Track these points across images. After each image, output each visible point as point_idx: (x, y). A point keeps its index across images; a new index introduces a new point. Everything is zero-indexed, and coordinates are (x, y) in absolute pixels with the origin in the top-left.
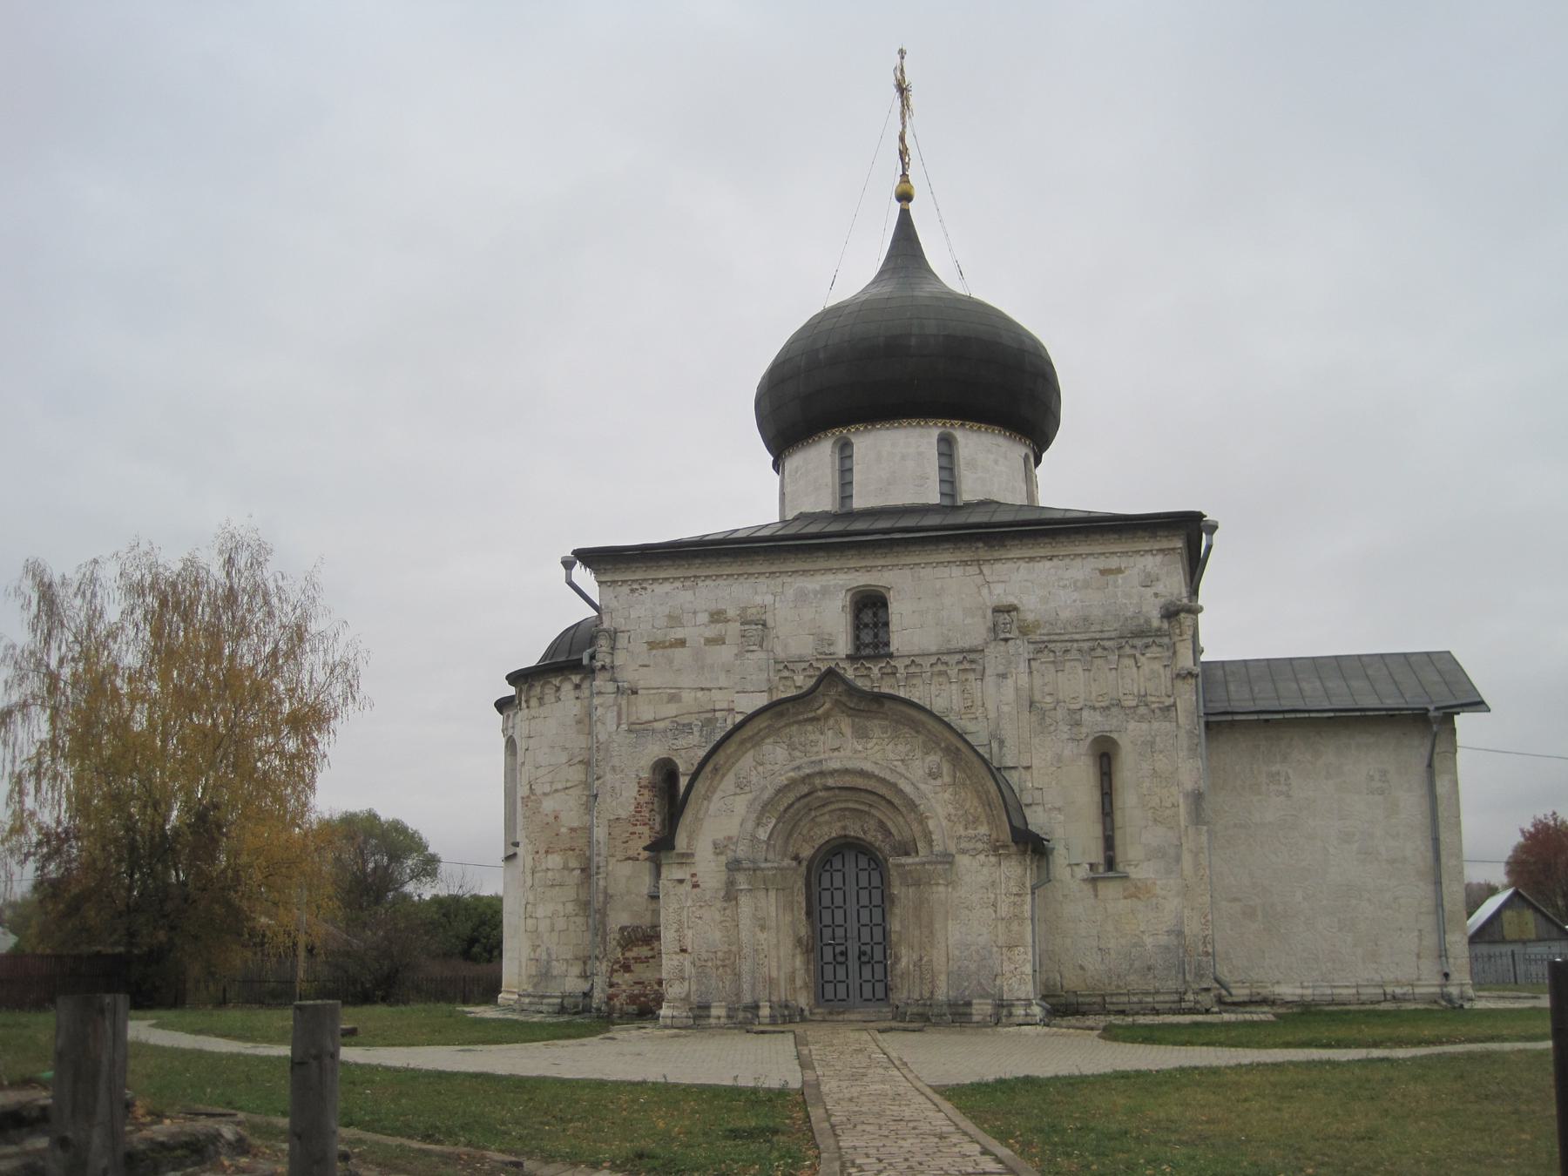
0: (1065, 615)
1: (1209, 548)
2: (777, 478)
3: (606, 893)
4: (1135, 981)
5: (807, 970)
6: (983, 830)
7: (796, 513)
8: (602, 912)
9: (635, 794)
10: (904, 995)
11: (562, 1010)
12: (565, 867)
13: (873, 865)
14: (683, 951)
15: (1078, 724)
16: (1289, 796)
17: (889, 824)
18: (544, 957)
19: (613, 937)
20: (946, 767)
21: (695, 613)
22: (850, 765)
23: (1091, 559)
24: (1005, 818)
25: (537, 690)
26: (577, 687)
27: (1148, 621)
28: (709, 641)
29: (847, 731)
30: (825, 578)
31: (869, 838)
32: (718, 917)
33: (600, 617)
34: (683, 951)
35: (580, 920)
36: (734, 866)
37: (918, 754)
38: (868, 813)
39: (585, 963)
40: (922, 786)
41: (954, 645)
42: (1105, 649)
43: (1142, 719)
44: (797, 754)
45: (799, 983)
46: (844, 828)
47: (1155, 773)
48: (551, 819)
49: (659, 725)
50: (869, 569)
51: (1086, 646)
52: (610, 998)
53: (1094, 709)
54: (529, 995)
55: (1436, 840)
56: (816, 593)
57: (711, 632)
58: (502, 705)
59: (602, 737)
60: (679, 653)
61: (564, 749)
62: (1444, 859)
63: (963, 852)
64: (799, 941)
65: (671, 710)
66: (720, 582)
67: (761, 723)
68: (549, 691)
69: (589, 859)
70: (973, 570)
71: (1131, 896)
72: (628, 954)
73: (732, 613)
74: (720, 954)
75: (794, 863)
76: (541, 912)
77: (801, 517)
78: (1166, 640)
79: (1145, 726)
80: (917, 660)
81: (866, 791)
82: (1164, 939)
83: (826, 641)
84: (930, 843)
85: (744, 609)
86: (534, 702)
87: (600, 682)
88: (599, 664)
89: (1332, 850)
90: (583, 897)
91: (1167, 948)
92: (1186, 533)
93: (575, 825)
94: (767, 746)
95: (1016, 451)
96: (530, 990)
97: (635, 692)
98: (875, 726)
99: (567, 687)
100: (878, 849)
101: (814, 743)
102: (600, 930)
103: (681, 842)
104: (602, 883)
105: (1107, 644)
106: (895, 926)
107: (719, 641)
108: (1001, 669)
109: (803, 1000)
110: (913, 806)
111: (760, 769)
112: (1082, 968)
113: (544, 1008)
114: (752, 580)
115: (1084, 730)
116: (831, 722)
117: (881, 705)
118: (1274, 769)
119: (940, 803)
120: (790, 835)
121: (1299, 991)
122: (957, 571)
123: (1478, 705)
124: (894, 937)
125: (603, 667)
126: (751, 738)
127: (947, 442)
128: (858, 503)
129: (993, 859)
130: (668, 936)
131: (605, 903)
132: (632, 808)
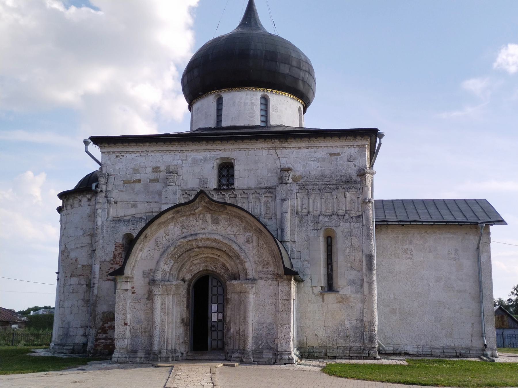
0: (313, 173)
1: (380, 144)
2: (190, 113)
3: (97, 296)
4: (341, 343)
5: (186, 334)
6: (271, 268)
7: (197, 128)
8: (94, 305)
9: (114, 250)
10: (231, 347)
11: (73, 352)
12: (79, 284)
13: (219, 284)
14: (126, 324)
15: (318, 222)
16: (411, 259)
17: (228, 265)
19: (99, 317)
20: (255, 238)
21: (146, 168)
22: (209, 236)
23: (326, 148)
24: (281, 263)
25: (71, 201)
26: (89, 200)
27: (351, 177)
28: (152, 181)
29: (209, 220)
30: (206, 153)
31: (218, 271)
32: (143, 308)
33: (101, 169)
34: (126, 324)
35: (85, 309)
36: (153, 282)
37: (242, 232)
38: (218, 260)
39: (85, 330)
40: (243, 247)
41: (262, 185)
42: (330, 189)
43: (347, 221)
44: (185, 230)
45: (181, 341)
46: (206, 266)
47: (352, 246)
48: (74, 261)
49: (127, 218)
50: (225, 150)
51: (322, 187)
52: (96, 346)
53: (325, 216)
55: (480, 282)
56: (201, 160)
57: (153, 176)
58: (59, 210)
59: (99, 223)
60: (138, 186)
61: (82, 228)
62: (484, 291)
63: (261, 278)
64: (183, 320)
65: (132, 211)
66: (158, 154)
67: (169, 215)
68: (76, 201)
69: (90, 280)
70: (272, 152)
71: (340, 302)
72: (106, 325)
73: (163, 168)
74: (143, 326)
75: (182, 283)
77: (199, 129)
78: (359, 186)
79: (348, 224)
80: (245, 191)
81: (217, 249)
82: (354, 322)
83: (203, 181)
84: (246, 274)
85: (168, 167)
86: (69, 207)
87: (101, 198)
88: (100, 190)
89: (431, 285)
90: (86, 298)
91: (356, 327)
92: (369, 136)
93: (85, 264)
94: (171, 226)
95: (296, 104)
97: (117, 203)
98: (222, 218)
99: (85, 200)
100: (222, 276)
101: (194, 226)
102: (93, 314)
103: (128, 271)
104: (96, 291)
105: (331, 186)
106: (228, 313)
107: (156, 180)
108: (284, 196)
109: (183, 349)
110: (238, 256)
111: (167, 237)
112: (316, 335)
113: (64, 351)
114: (172, 153)
115: (319, 225)
116: (202, 216)
117: (226, 209)
118: (406, 247)
119: (252, 256)
120: (181, 269)
121: (416, 350)
122: (265, 152)
123: (501, 221)
124: (228, 319)
125: (101, 191)
126: (163, 223)
127: (265, 101)
128: (224, 124)
129: (275, 283)
130: (118, 317)
131: (96, 301)
132: (112, 256)
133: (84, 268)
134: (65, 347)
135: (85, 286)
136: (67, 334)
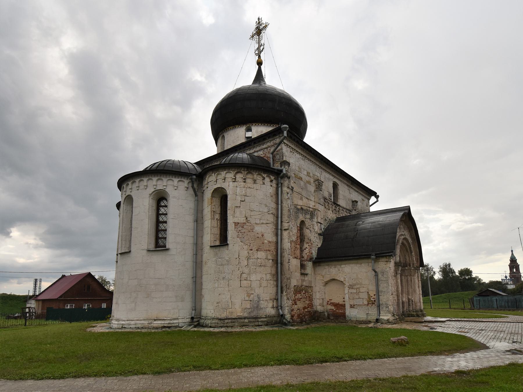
18: (256, 299)
26: (271, 181)
48: (260, 236)
54: (245, 318)
76: (253, 277)
86: (249, 181)
93: (271, 240)
96: (246, 315)
133: (270, 244)
134: (259, 320)
135: (271, 261)
136: (257, 307)
